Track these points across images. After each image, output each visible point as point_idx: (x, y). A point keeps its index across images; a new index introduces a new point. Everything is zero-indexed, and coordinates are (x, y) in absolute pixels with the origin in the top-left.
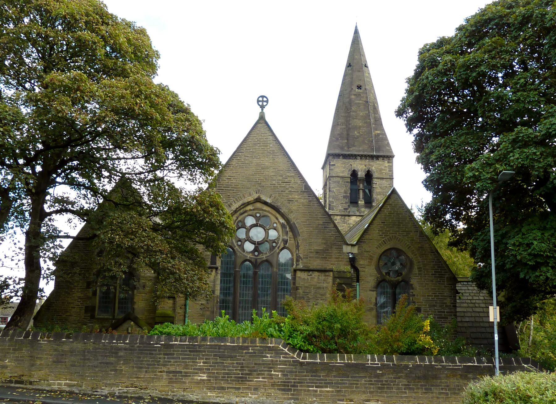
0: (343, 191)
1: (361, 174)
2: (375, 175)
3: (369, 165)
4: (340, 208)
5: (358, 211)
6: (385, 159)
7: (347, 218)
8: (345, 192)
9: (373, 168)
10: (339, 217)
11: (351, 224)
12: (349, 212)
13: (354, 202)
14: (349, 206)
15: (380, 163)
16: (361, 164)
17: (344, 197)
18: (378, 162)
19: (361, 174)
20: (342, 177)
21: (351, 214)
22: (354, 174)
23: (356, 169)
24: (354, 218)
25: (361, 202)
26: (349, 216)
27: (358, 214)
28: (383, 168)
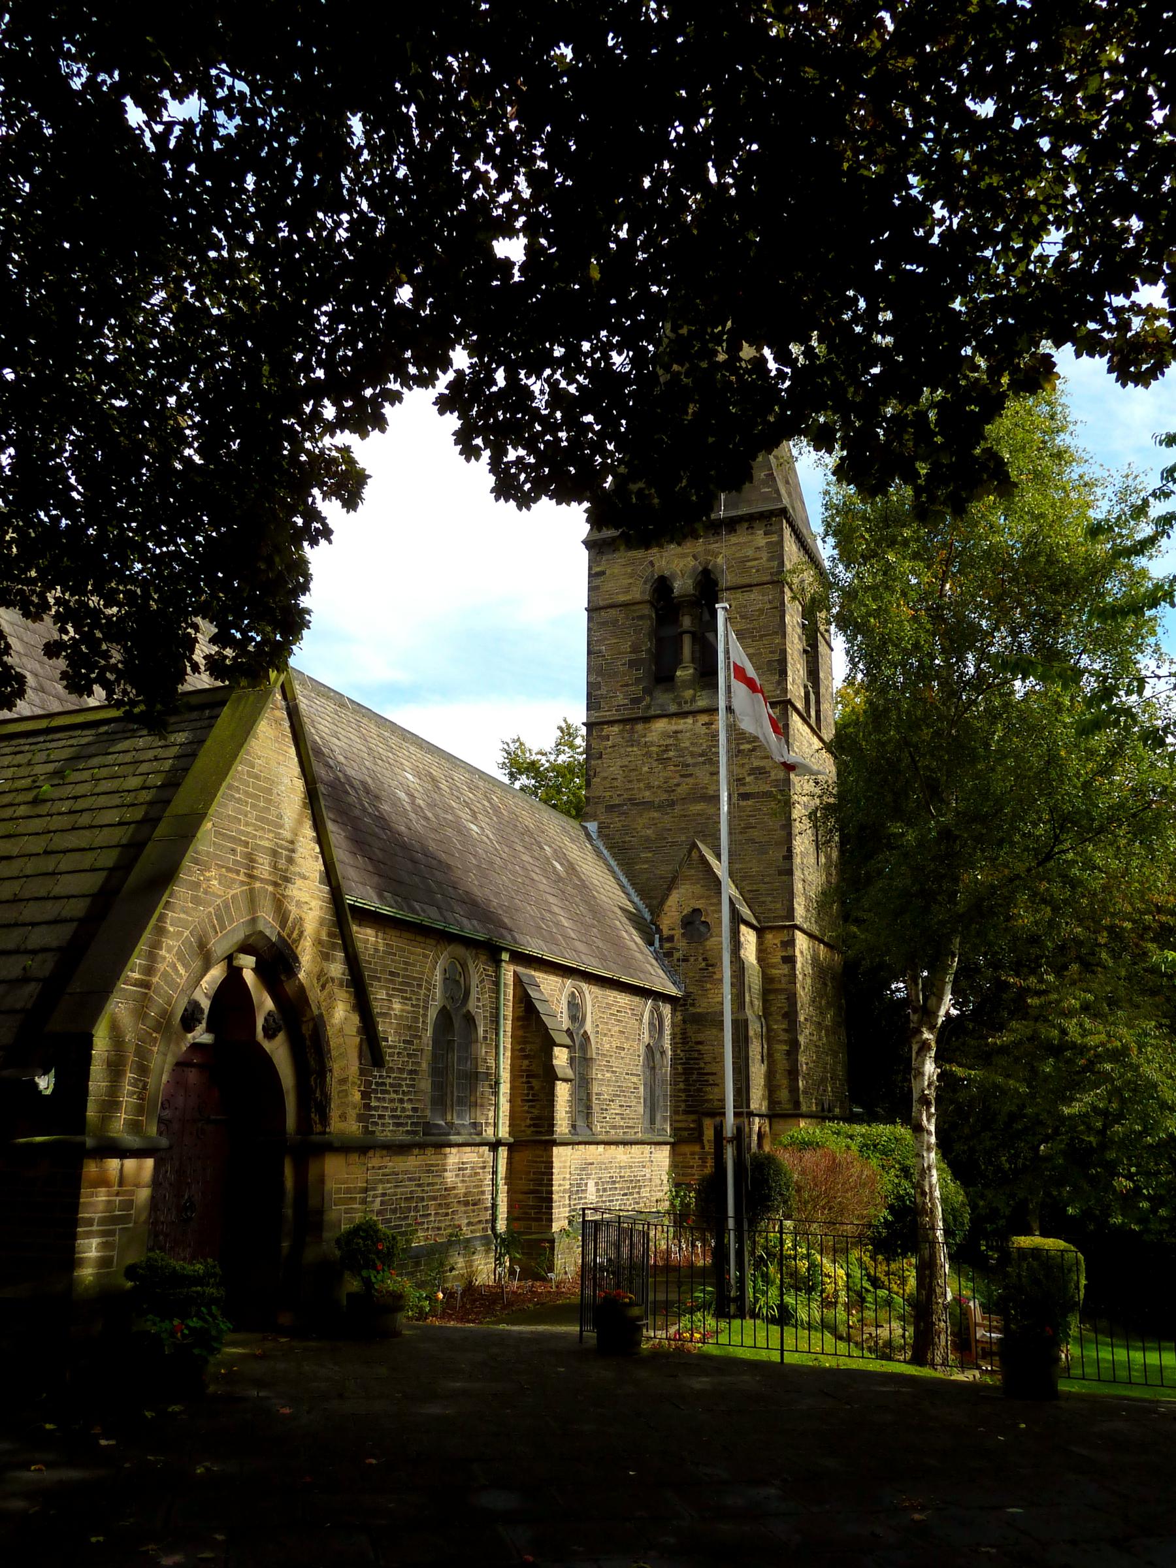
0: (626, 646)
1: (682, 585)
2: (727, 579)
3: (707, 552)
4: (621, 699)
5: (674, 700)
6: (757, 524)
7: (639, 727)
8: (635, 649)
9: (720, 560)
10: (616, 729)
11: (652, 744)
12: (648, 707)
13: (663, 677)
14: (648, 691)
15: (742, 540)
16: (684, 556)
17: (632, 664)
18: (734, 539)
19: (682, 585)
20: (625, 605)
21: (652, 712)
22: (662, 586)
23: (667, 573)
24: (661, 725)
25: (684, 673)
26: (647, 719)
27: (673, 708)
28: (750, 553)
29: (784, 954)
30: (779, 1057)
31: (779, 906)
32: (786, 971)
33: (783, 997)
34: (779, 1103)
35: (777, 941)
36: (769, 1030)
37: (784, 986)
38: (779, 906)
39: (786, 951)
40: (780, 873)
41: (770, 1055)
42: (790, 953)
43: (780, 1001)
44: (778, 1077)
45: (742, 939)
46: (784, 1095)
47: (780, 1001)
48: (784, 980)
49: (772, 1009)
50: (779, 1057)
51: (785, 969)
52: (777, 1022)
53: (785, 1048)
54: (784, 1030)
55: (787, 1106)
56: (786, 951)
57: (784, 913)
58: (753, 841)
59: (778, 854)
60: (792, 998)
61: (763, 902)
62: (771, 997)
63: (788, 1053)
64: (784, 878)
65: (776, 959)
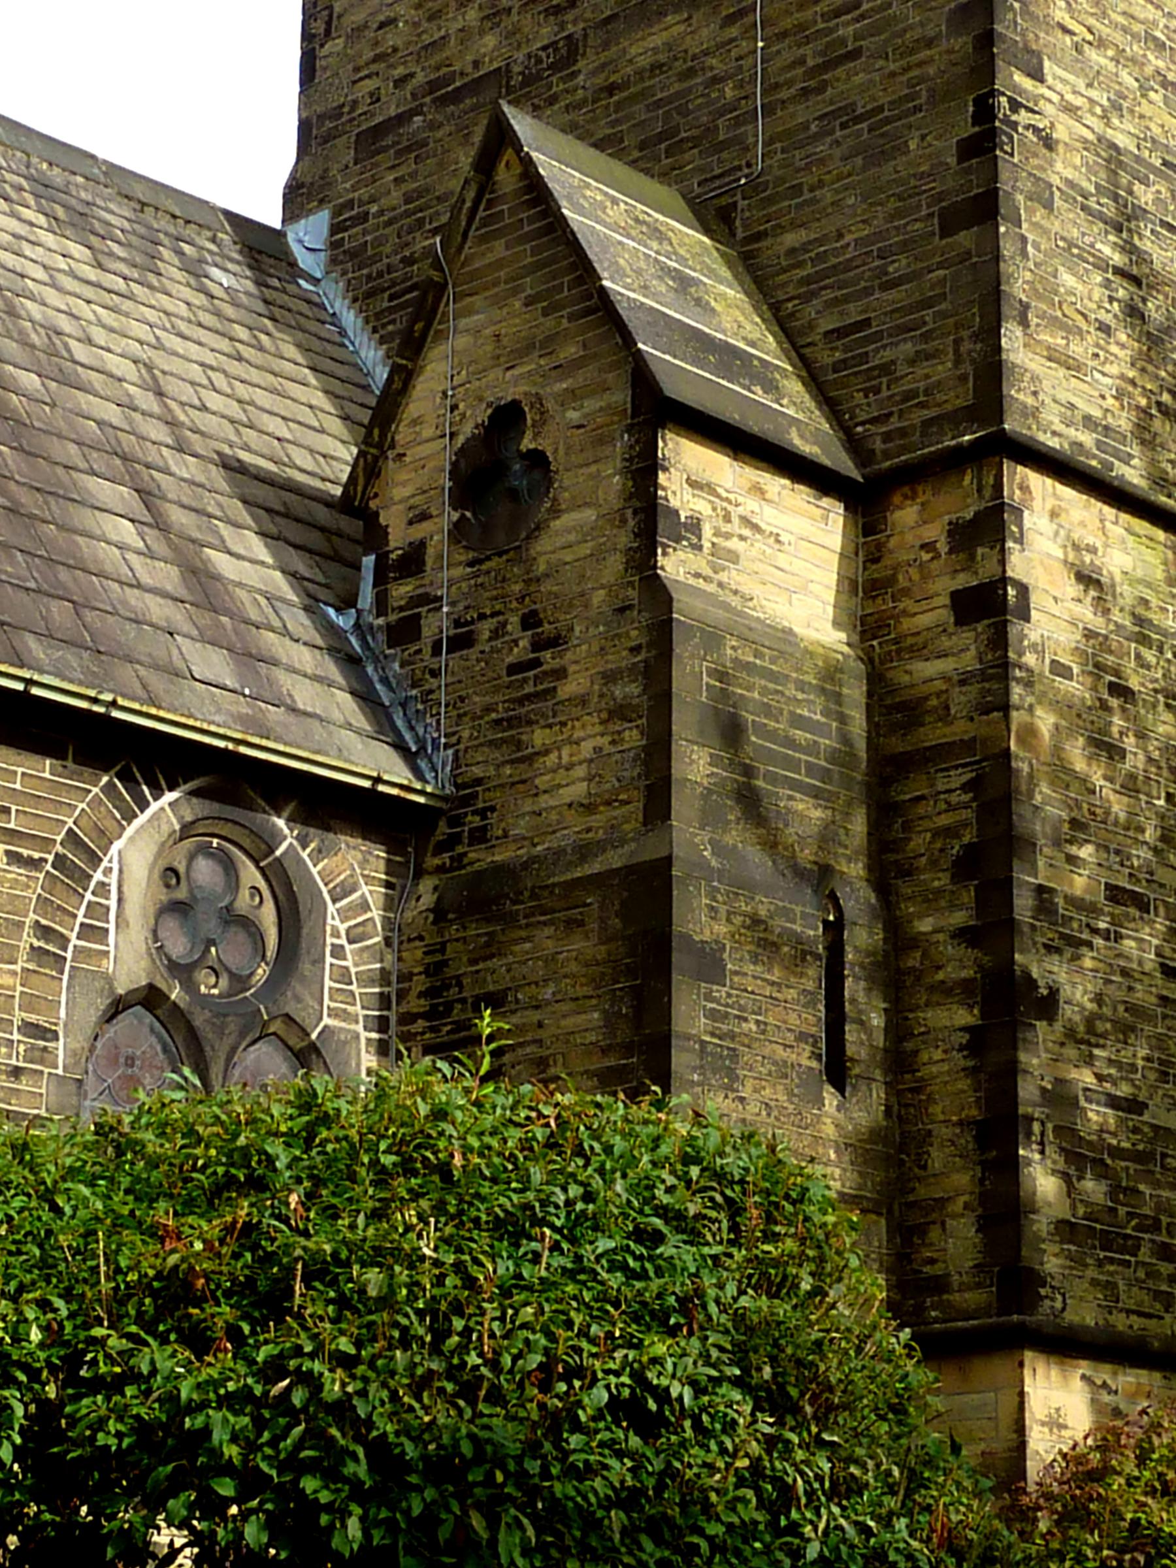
29: (963, 581)
30: (941, 1064)
31: (943, 369)
32: (969, 661)
33: (959, 777)
34: (940, 1285)
35: (936, 532)
36: (898, 936)
37: (960, 730)
38: (943, 369)
39: (970, 564)
40: (951, 221)
41: (899, 1060)
42: (986, 570)
43: (943, 804)
44: (937, 1158)
45: (674, 490)
46: (957, 1244)
47: (943, 804)
48: (961, 700)
49: (918, 842)
50: (941, 1064)
51: (966, 650)
52: (931, 900)
53: (964, 1017)
54: (963, 935)
55: (973, 1298)
56: (970, 564)
57: (958, 398)
58: (847, 116)
59: (932, 146)
60: (995, 787)
61: (886, 369)
62: (915, 787)
63: (977, 1042)
64: (965, 238)
65: (929, 614)
